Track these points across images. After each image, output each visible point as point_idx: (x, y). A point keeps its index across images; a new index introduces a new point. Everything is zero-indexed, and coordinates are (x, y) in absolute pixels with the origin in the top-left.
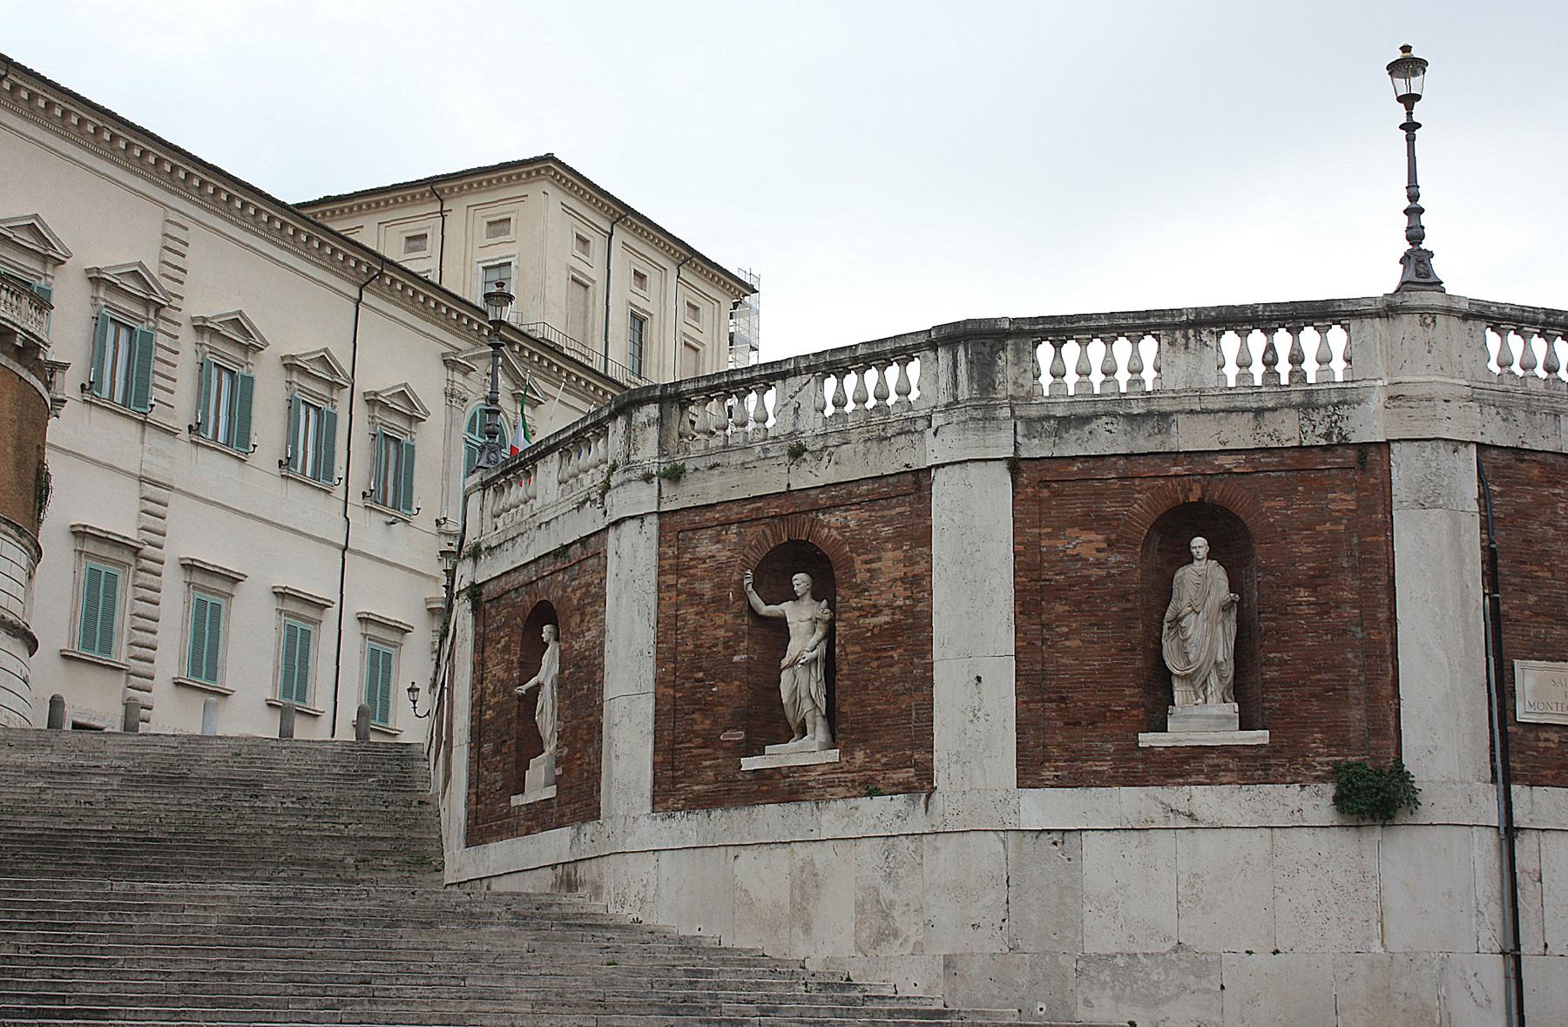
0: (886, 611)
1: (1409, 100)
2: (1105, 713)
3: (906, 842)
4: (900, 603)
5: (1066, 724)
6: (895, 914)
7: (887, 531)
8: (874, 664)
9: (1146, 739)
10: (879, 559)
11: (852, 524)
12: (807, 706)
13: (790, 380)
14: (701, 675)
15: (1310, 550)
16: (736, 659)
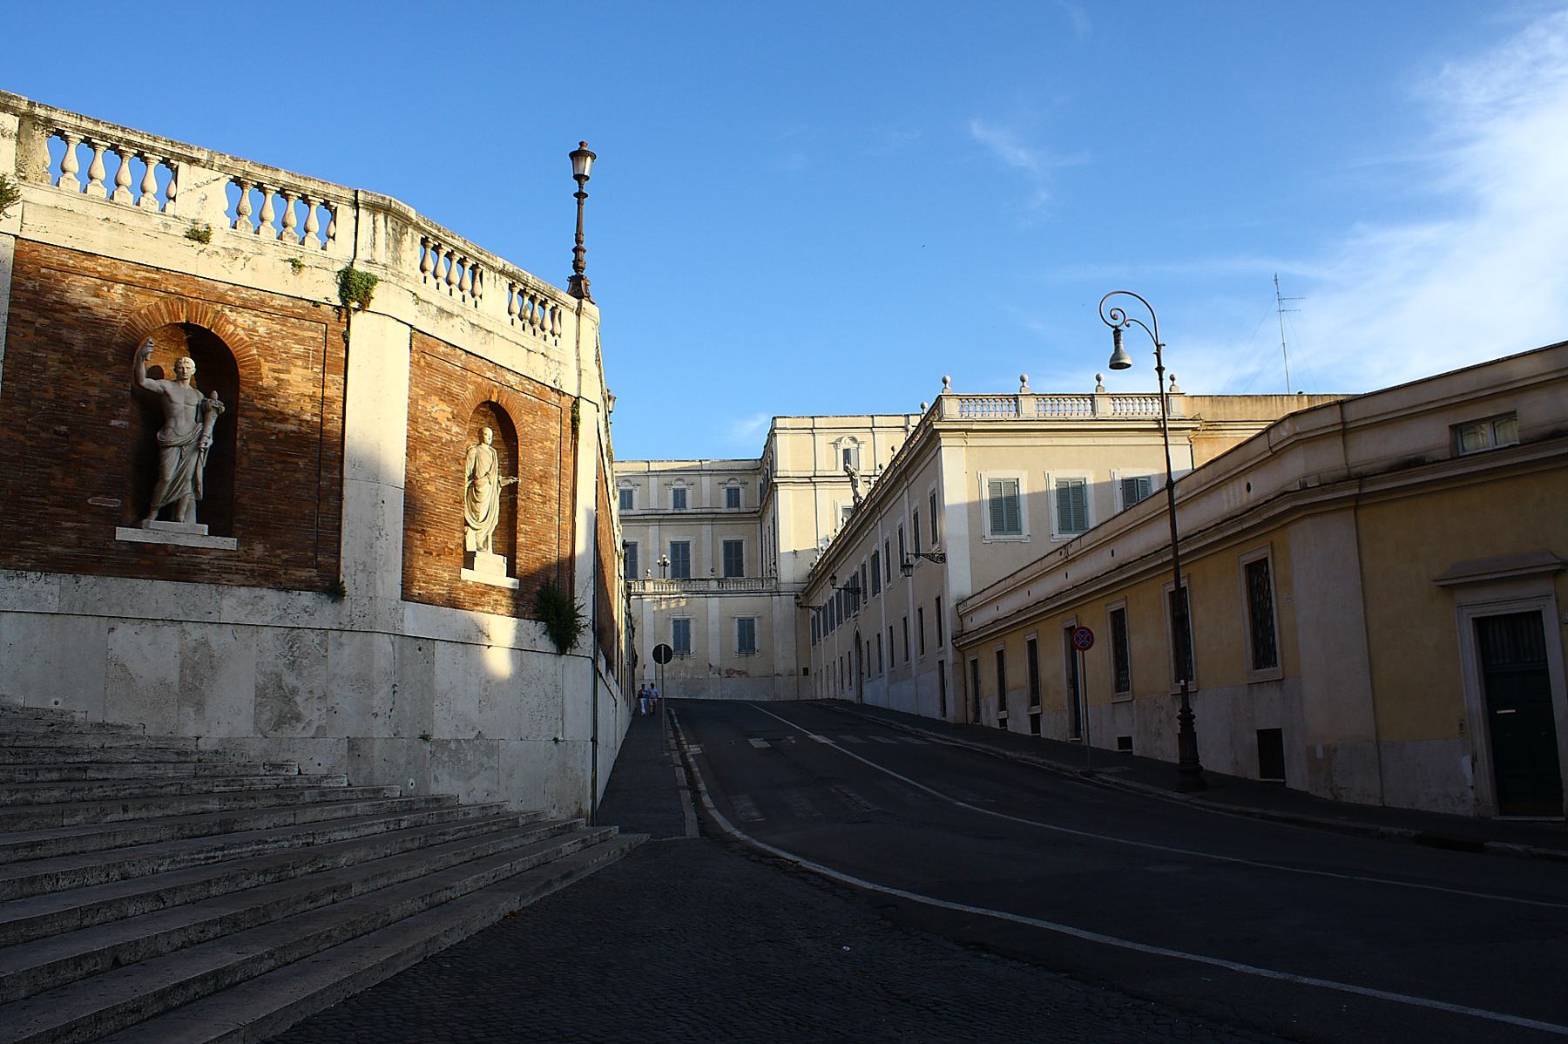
0: (293, 421)
1: (580, 178)
2: (444, 549)
3: (312, 635)
4: (307, 417)
5: (425, 552)
6: (298, 699)
7: (297, 349)
8: (278, 466)
9: (466, 574)
10: (288, 372)
11: (262, 330)
12: (189, 488)
13: (196, 169)
14: (63, 428)
15: (541, 457)
16: (114, 423)
